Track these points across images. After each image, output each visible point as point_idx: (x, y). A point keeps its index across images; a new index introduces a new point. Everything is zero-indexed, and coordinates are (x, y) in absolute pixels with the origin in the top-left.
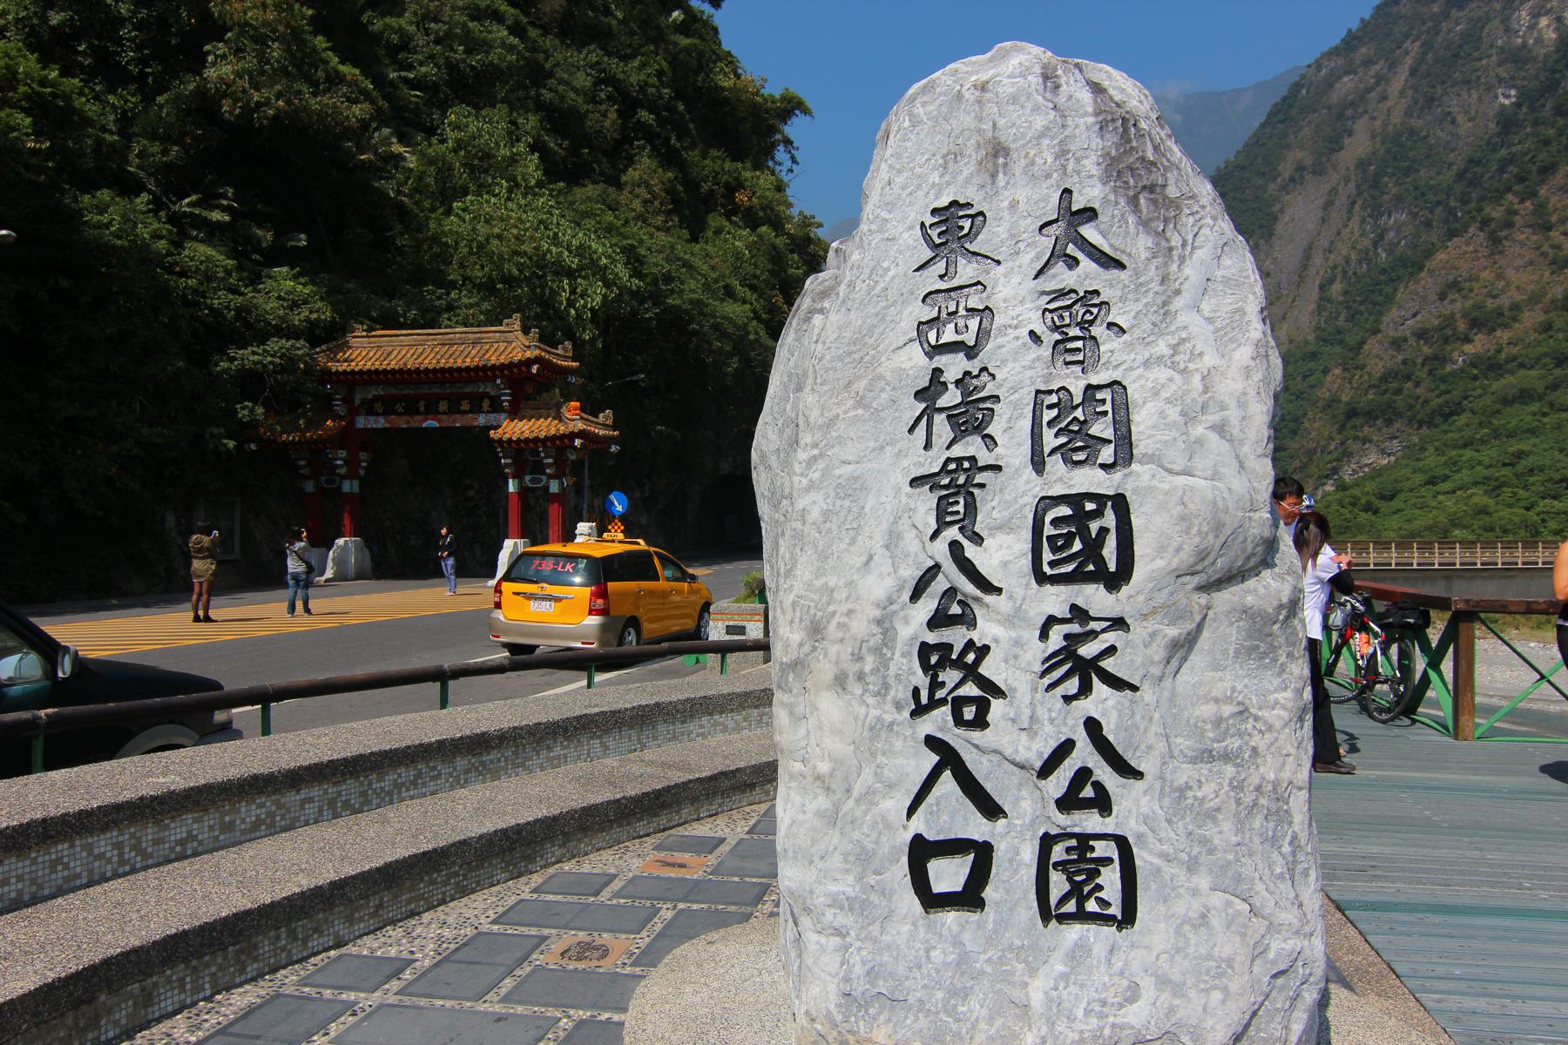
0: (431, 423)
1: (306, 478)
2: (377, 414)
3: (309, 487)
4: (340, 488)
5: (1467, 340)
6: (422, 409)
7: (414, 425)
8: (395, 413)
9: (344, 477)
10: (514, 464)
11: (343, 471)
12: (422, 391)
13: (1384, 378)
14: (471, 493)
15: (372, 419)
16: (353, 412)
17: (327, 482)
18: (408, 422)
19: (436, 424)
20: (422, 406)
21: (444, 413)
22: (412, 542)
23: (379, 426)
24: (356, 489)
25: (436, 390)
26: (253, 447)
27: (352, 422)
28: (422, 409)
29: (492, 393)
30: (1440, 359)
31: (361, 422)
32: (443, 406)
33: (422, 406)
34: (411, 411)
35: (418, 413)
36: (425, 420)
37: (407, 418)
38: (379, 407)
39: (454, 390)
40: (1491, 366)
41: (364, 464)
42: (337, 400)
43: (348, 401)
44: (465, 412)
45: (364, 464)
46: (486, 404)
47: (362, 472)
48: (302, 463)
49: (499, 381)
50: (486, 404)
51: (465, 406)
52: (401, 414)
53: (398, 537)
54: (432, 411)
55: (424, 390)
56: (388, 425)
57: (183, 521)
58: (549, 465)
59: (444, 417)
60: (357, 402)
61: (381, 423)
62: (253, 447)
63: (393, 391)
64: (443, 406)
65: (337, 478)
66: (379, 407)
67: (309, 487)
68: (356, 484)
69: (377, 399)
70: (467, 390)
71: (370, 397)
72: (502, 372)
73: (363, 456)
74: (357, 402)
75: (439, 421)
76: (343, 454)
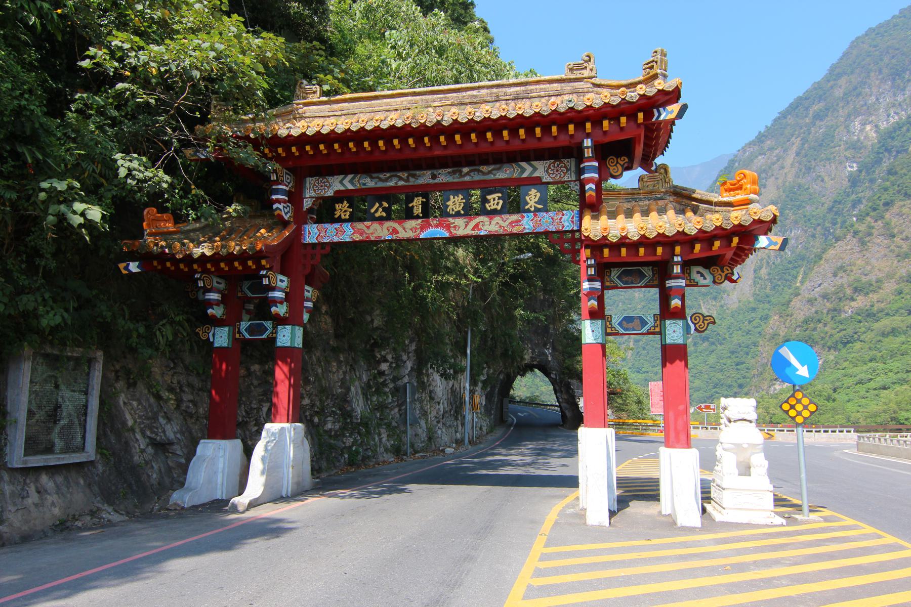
1: (217, 322)
2: (340, 220)
3: (221, 338)
4: (273, 340)
5: (853, 299)
7: (403, 235)
8: (374, 219)
11: (281, 310)
12: (421, 181)
13: (806, 322)
15: (331, 228)
16: (301, 218)
17: (250, 330)
20: (417, 204)
21: (458, 215)
22: (329, 426)
23: (346, 238)
24: (299, 343)
26: (134, 267)
28: (418, 210)
30: (836, 311)
33: (417, 204)
35: (409, 215)
36: (423, 228)
38: (343, 209)
39: (477, 177)
40: (870, 315)
42: (277, 192)
43: (295, 198)
44: (494, 213)
45: (309, 304)
47: (306, 317)
48: (214, 296)
50: (533, 197)
51: (495, 201)
52: (381, 219)
53: (316, 420)
56: (358, 238)
59: (460, 222)
60: (307, 204)
62: (134, 267)
63: (370, 183)
66: (343, 209)
67: (221, 338)
68: (299, 332)
69: (340, 197)
70: (501, 175)
71: (330, 193)
72: (597, 123)
73: (309, 292)
74: (307, 204)
75: (448, 227)
76: (282, 281)
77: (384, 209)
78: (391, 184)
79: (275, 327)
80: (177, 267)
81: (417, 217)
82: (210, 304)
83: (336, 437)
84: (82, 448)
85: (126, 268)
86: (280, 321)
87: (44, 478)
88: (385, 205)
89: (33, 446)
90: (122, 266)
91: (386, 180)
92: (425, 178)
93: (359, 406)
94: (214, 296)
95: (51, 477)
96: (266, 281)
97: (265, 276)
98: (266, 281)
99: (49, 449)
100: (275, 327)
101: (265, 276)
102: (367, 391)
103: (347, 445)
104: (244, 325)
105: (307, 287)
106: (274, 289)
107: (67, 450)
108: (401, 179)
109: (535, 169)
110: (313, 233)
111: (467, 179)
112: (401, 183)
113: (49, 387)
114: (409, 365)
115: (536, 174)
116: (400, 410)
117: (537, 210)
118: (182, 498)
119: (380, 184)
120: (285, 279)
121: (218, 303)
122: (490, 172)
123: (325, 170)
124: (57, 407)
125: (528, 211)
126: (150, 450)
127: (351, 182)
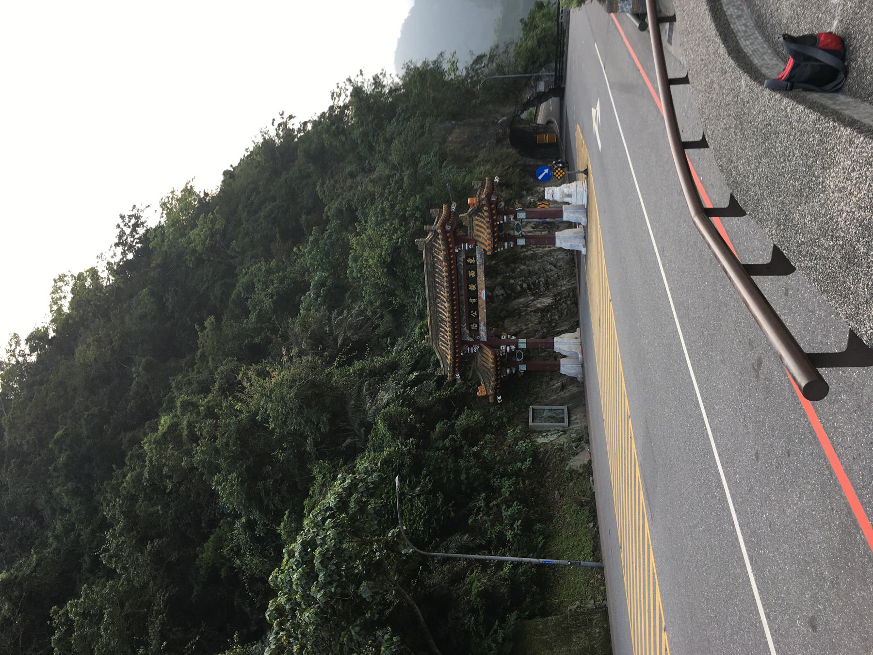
0: (483, 294)
2: (478, 328)
6: (474, 300)
7: (484, 305)
8: (477, 316)
9: (517, 346)
10: (508, 242)
11: (513, 347)
14: (525, 286)
16: (477, 342)
18: (483, 309)
19: (484, 292)
21: (476, 287)
25: (463, 292)
26: (499, 398)
27: (484, 343)
28: (474, 300)
29: (464, 257)
31: (483, 335)
32: (472, 287)
34: (475, 307)
35: (477, 303)
37: (480, 309)
41: (509, 337)
42: (470, 350)
43: (470, 345)
44: (476, 274)
46: (470, 261)
48: (508, 371)
49: (457, 251)
50: (470, 261)
52: (478, 313)
53: (554, 324)
54: (475, 294)
55: (463, 298)
57: (545, 434)
58: (509, 219)
59: (479, 287)
60: (471, 339)
61: (483, 328)
64: (472, 287)
65: (518, 351)
66: (474, 327)
67: (523, 368)
68: (520, 340)
69: (469, 328)
71: (468, 331)
73: (504, 337)
74: (471, 339)
76: (503, 347)
77: (474, 312)
78: (465, 310)
79: (519, 349)
80: (499, 383)
81: (477, 301)
82: (511, 372)
83: (562, 314)
84: (563, 410)
85: (500, 400)
86: (517, 348)
87: (572, 419)
88: (472, 312)
89: (562, 420)
90: (499, 401)
91: (463, 312)
92: (463, 298)
93: (547, 301)
94: (508, 371)
95: (572, 417)
96: (504, 353)
97: (502, 353)
98: (504, 353)
99: (563, 418)
100: (519, 349)
101: (502, 353)
102: (538, 295)
103: (566, 307)
104: (518, 360)
105: (502, 338)
106: (506, 351)
107: (563, 413)
108: (463, 307)
109: (460, 261)
110: (483, 335)
111: (463, 284)
112: (464, 307)
113: (543, 419)
114: (523, 267)
115: (462, 260)
116: (548, 271)
117: (475, 259)
118: (579, 377)
119: (465, 314)
120: (501, 347)
121: (511, 370)
122: (461, 276)
123: (461, 334)
124: (549, 416)
125: (476, 262)
126: (564, 391)
127: (463, 324)
